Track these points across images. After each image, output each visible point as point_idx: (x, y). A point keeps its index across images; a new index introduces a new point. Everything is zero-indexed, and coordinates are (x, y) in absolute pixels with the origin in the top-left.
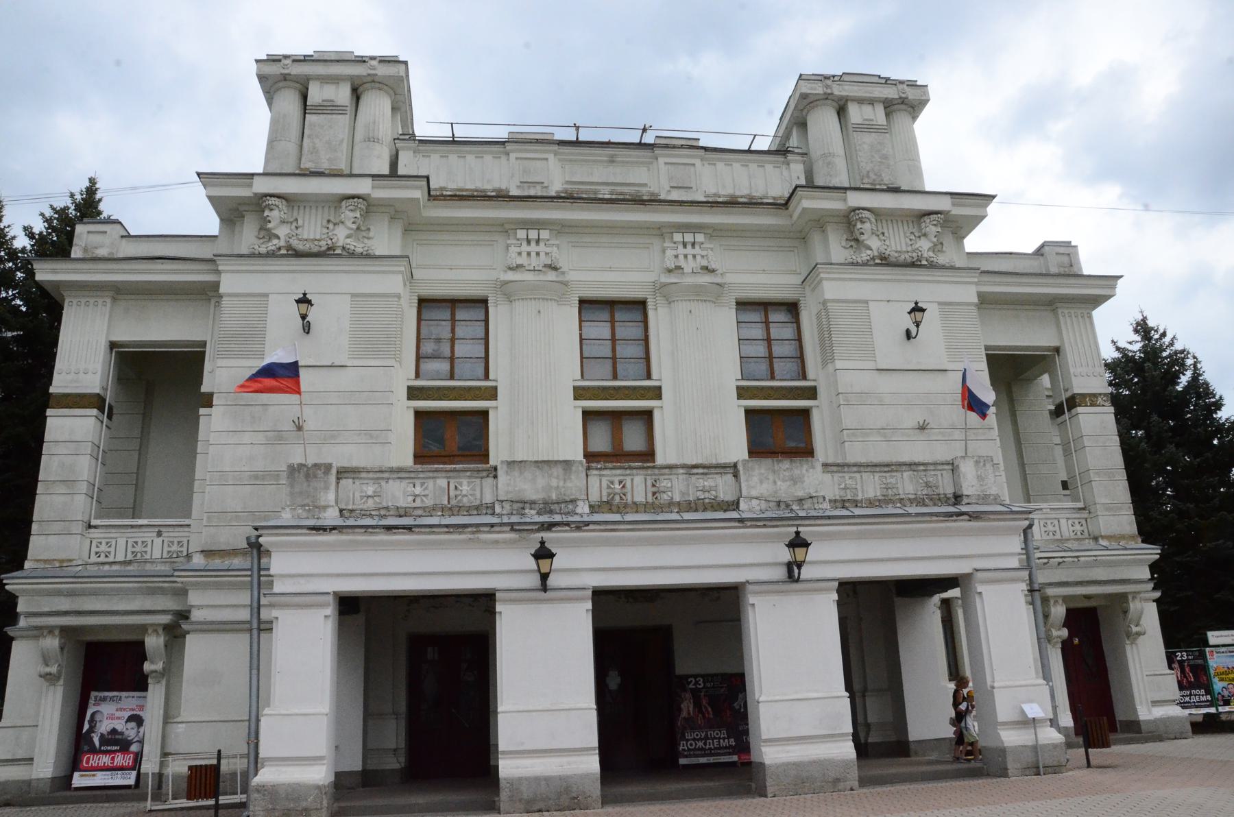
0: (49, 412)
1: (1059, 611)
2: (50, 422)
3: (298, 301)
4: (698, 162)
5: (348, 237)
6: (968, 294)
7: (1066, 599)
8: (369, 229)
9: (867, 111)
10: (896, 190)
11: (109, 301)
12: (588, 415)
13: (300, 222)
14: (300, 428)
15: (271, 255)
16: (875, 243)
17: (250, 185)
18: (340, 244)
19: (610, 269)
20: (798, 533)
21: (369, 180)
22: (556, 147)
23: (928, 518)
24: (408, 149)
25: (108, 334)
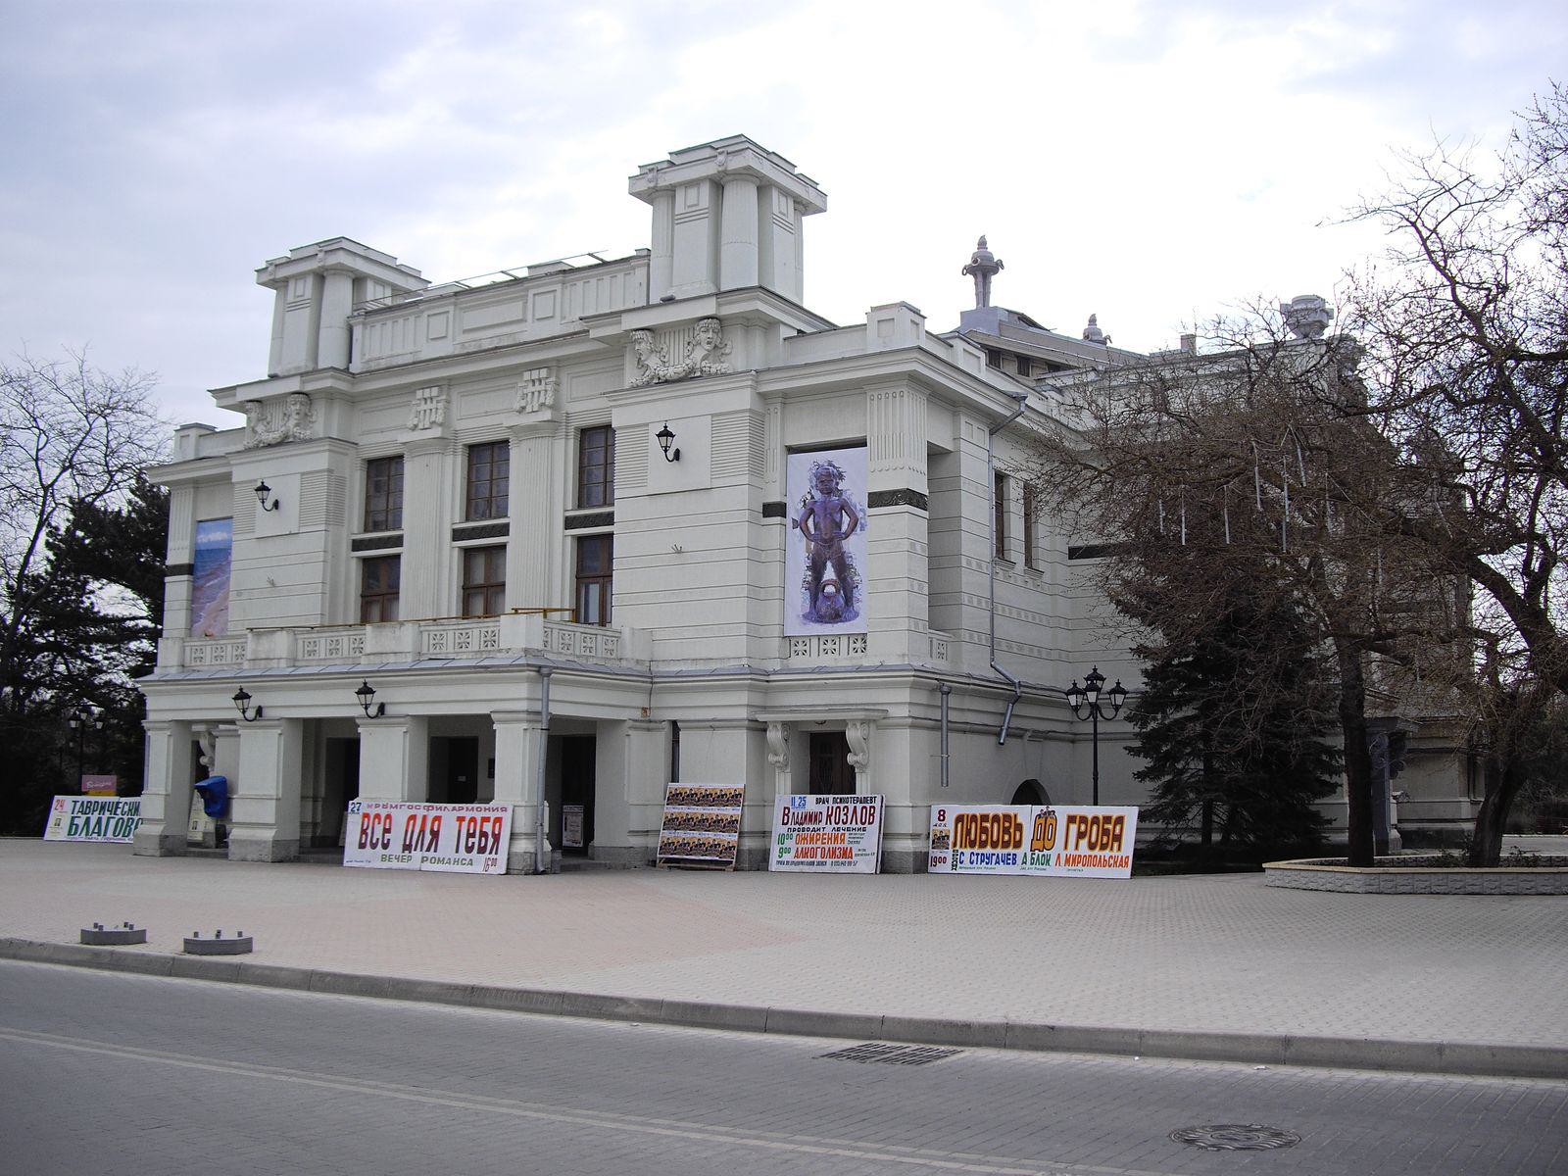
0: (167, 579)
1: (774, 736)
2: (168, 588)
3: (257, 490)
4: (558, 287)
5: (297, 425)
6: (742, 399)
7: (785, 724)
8: (312, 415)
9: (692, 192)
10: (669, 301)
11: (192, 490)
12: (468, 553)
13: (269, 419)
14: (273, 584)
15: (257, 448)
16: (653, 362)
17: (235, 395)
18: (291, 433)
19: (487, 414)
20: (365, 684)
21: (298, 378)
22: (453, 300)
23: (473, 670)
24: (359, 323)
25: (194, 513)
